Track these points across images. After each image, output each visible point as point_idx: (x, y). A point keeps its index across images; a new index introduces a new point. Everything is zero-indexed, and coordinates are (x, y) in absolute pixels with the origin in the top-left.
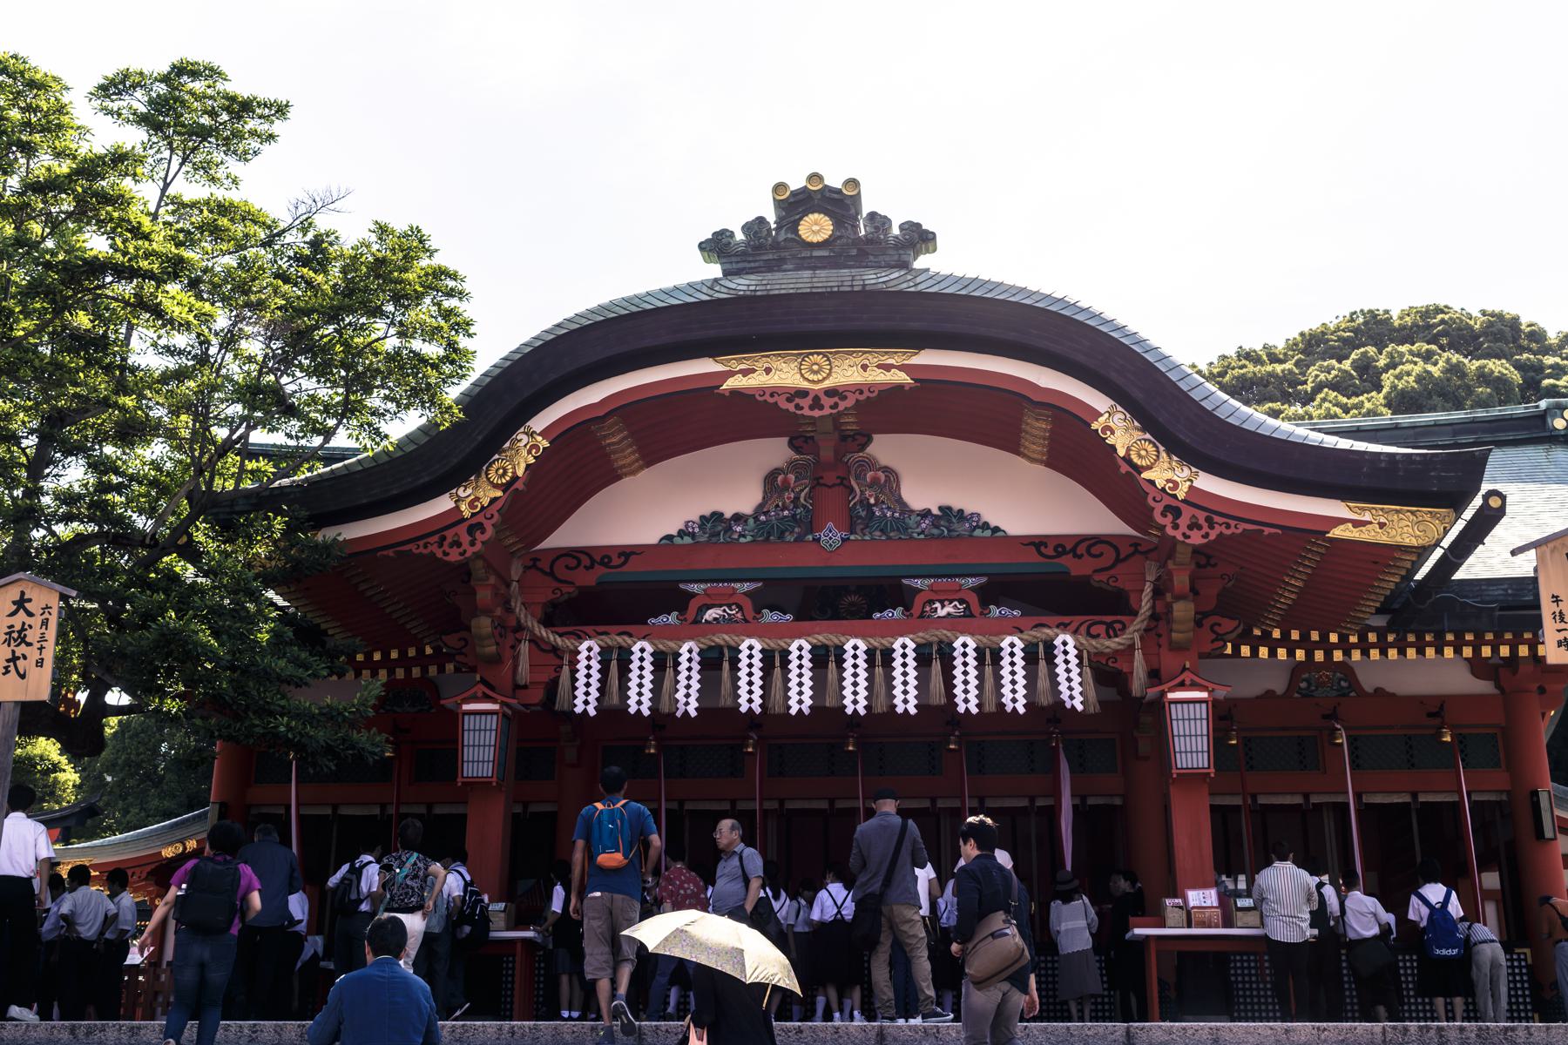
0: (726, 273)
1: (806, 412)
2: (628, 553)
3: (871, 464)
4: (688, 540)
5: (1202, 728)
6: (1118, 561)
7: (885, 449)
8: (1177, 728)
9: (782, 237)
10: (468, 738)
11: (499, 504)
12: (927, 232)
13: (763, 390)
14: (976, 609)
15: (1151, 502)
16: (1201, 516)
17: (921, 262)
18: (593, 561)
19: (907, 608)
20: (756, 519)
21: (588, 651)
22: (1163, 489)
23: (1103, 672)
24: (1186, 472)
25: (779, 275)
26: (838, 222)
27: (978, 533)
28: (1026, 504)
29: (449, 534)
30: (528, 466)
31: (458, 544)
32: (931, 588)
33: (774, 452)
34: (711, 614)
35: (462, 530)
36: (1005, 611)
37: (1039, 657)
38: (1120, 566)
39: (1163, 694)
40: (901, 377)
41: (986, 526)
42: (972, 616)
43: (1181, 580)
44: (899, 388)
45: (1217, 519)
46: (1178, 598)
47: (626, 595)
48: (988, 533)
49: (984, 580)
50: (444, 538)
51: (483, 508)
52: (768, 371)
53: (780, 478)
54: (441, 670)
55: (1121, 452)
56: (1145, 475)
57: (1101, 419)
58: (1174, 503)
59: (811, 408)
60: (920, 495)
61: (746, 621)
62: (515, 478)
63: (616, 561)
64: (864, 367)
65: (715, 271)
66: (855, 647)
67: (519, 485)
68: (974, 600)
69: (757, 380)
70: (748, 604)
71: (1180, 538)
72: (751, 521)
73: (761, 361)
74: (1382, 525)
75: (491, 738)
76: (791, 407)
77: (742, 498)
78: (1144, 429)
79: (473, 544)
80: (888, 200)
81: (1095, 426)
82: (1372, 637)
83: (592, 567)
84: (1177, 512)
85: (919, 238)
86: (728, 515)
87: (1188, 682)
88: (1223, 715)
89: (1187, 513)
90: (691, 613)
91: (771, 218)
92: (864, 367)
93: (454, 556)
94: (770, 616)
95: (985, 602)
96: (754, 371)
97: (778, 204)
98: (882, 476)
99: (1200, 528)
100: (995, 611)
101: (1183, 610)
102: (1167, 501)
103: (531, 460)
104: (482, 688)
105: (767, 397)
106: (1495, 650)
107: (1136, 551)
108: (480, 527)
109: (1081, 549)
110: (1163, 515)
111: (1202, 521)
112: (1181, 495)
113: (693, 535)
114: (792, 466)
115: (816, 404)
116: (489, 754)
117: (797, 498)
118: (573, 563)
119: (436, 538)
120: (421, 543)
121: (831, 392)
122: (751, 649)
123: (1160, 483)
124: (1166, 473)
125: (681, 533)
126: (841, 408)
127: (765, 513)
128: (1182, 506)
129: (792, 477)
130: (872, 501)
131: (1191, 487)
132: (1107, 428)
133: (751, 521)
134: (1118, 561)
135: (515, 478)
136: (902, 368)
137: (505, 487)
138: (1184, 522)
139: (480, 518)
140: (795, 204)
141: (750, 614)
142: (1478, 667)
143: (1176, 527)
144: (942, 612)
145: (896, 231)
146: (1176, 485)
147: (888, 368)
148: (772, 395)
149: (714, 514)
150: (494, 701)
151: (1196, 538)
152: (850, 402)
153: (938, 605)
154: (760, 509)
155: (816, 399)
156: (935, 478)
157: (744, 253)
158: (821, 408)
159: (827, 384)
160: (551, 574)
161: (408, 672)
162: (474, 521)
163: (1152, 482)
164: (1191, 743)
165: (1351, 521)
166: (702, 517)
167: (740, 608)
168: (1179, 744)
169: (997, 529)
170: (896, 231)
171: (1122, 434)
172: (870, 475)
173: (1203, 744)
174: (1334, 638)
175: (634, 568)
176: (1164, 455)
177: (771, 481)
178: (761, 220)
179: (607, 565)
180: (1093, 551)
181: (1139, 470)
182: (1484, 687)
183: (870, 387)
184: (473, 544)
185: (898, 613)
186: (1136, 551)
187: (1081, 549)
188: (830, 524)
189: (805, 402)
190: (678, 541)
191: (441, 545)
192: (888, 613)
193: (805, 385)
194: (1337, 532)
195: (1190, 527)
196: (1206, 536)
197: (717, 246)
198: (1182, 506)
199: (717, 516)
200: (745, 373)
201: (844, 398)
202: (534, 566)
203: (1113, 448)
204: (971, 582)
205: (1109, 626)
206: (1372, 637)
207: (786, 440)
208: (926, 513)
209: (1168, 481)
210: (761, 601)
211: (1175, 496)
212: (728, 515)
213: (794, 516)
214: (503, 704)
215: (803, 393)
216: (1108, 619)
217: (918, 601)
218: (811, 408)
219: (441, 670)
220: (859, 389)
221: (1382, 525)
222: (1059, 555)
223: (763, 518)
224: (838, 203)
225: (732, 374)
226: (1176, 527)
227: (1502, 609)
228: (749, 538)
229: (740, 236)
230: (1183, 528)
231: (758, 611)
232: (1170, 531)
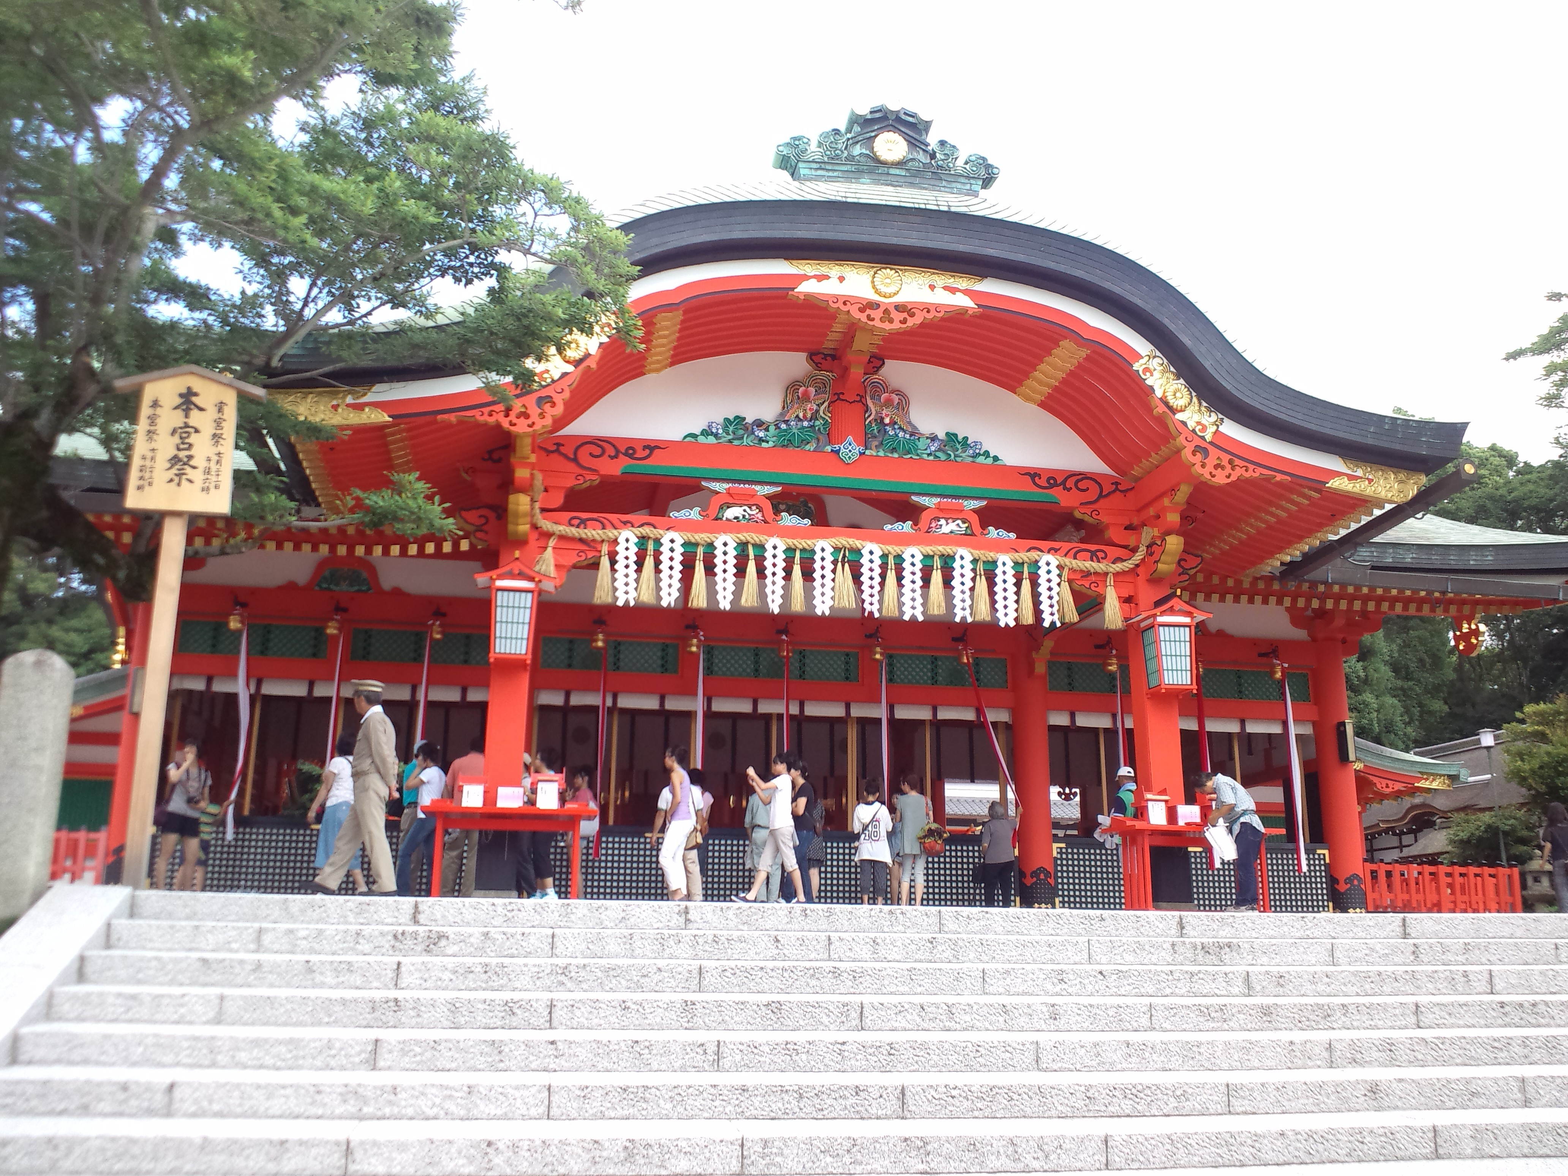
1: (877, 323)
2: (652, 447)
3: (884, 387)
4: (711, 440)
5: (1186, 649)
6: (1101, 496)
7: (895, 372)
8: (1165, 648)
10: (500, 614)
11: (568, 381)
12: (990, 166)
13: (837, 298)
14: (977, 529)
16: (1225, 458)
18: (618, 451)
19: (916, 523)
20: (777, 427)
22: (1194, 431)
24: (1214, 417)
27: (981, 460)
28: (1025, 440)
31: (526, 416)
32: (939, 507)
33: (795, 363)
36: (1003, 533)
37: (1027, 576)
38: (1102, 501)
40: (965, 302)
41: (987, 454)
42: (973, 534)
43: (1173, 518)
45: (1237, 462)
47: (644, 488)
48: (990, 461)
49: (984, 503)
51: (553, 381)
52: (841, 279)
53: (801, 390)
54: (386, 552)
55: (1159, 393)
56: (1179, 416)
57: (1142, 361)
58: (1203, 444)
60: (929, 420)
61: (766, 522)
62: (587, 356)
63: (640, 454)
64: (932, 287)
70: (768, 506)
72: (772, 428)
73: (834, 270)
74: (1370, 481)
76: (863, 317)
77: (764, 407)
78: (1178, 376)
79: (542, 416)
80: (956, 130)
81: (1136, 366)
82: (1261, 585)
83: (616, 457)
86: (749, 420)
87: (1176, 608)
88: (1205, 641)
90: (713, 511)
94: (788, 520)
95: (984, 526)
96: (827, 277)
98: (896, 399)
99: (1223, 468)
101: (1174, 543)
103: (605, 339)
105: (840, 305)
106: (1308, 602)
107: (1117, 489)
108: (549, 400)
109: (1070, 483)
110: (1194, 453)
111: (1225, 462)
112: (1209, 437)
113: (716, 436)
114: (809, 380)
117: (817, 411)
118: (597, 451)
119: (501, 407)
120: (486, 410)
121: (900, 308)
122: (776, 548)
123: (1191, 424)
124: (1195, 417)
125: (705, 433)
126: (911, 322)
127: (786, 422)
128: (1210, 448)
129: (812, 390)
130: (887, 421)
131: (1217, 432)
132: (1146, 370)
133: (772, 428)
134: (1101, 496)
135: (587, 356)
136: (966, 292)
137: (577, 363)
138: (1211, 461)
142: (1297, 618)
143: (1203, 466)
145: (960, 162)
147: (953, 290)
148: (845, 303)
149: (737, 417)
151: (1220, 479)
152: (917, 320)
153: (943, 522)
155: (886, 311)
156: (941, 407)
158: (891, 321)
160: (575, 460)
161: (351, 549)
162: (543, 393)
163: (1184, 423)
165: (1344, 477)
166: (727, 420)
167: (761, 510)
168: (1166, 663)
169: (996, 458)
170: (960, 162)
172: (884, 396)
173: (1186, 663)
174: (1230, 583)
175: (656, 466)
176: (1195, 400)
177: (793, 391)
178: (836, 132)
179: (631, 457)
180: (1080, 485)
181: (1174, 411)
182: (1301, 634)
183: (937, 307)
184: (542, 416)
186: (1117, 489)
187: (1070, 483)
188: (850, 438)
189: (877, 314)
190: (702, 439)
191: (507, 416)
193: (876, 298)
194: (1334, 483)
195: (1216, 467)
196: (1228, 477)
198: (1210, 448)
199: (739, 420)
201: (912, 315)
202: (557, 451)
206: (1261, 585)
207: (803, 355)
208: (933, 438)
209: (1199, 423)
211: (1203, 438)
212: (749, 420)
213: (813, 426)
215: (872, 305)
217: (925, 517)
219: (386, 552)
221: (1370, 481)
222: (1051, 486)
223: (784, 426)
224: (912, 127)
225: (806, 278)
226: (1203, 466)
227: (1373, 568)
228: (771, 444)
230: (1209, 468)
232: (1198, 469)
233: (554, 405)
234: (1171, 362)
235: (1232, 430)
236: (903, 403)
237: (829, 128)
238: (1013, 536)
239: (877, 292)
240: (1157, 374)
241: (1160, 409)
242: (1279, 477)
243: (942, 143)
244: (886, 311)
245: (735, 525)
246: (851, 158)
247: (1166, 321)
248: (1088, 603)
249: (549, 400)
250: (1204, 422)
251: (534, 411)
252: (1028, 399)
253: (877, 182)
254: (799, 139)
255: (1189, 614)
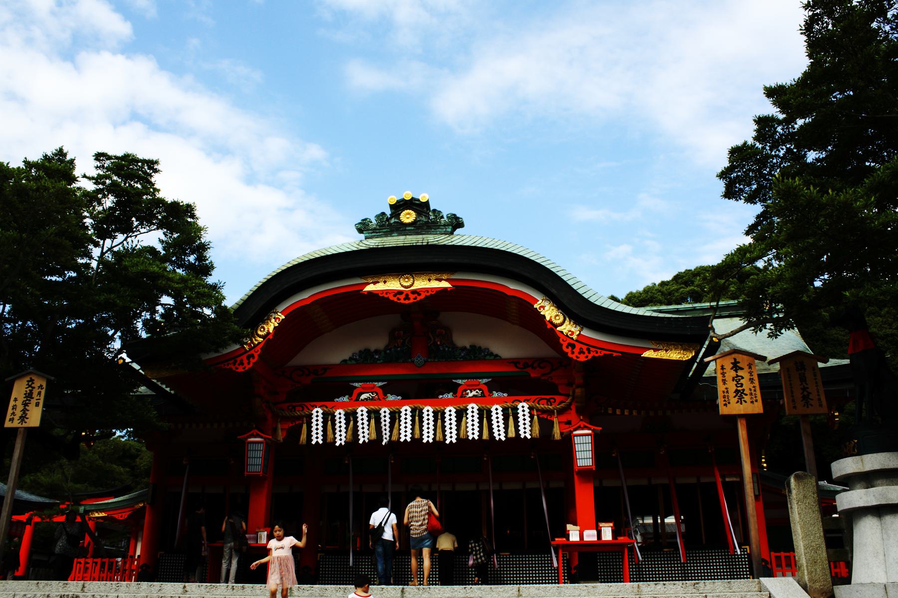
0: (366, 238)
1: (402, 301)
2: (327, 368)
4: (353, 362)
5: (589, 447)
7: (446, 318)
8: (578, 448)
9: (393, 221)
11: (260, 346)
14: (487, 393)
15: (561, 341)
16: (585, 348)
17: (458, 231)
19: (455, 393)
21: (317, 413)
23: (544, 421)
24: (578, 328)
25: (389, 238)
26: (419, 213)
27: (488, 357)
29: (239, 359)
30: (275, 328)
31: (242, 363)
34: (363, 396)
35: (244, 357)
36: (500, 394)
39: (572, 432)
40: (445, 284)
44: (445, 289)
45: (592, 349)
46: (577, 387)
50: (236, 361)
52: (385, 282)
55: (548, 318)
56: (559, 329)
59: (405, 299)
60: (463, 341)
62: (268, 333)
64: (429, 280)
65: (362, 236)
66: (428, 411)
67: (271, 337)
68: (485, 388)
69: (380, 287)
70: (380, 391)
71: (575, 358)
75: (260, 454)
76: (395, 299)
77: (378, 343)
79: (249, 363)
80: (443, 204)
81: (536, 306)
84: (573, 346)
85: (456, 223)
86: (372, 349)
89: (578, 346)
91: (388, 212)
92: (429, 280)
93: (241, 369)
94: (391, 398)
95: (491, 392)
97: (392, 206)
100: (495, 394)
102: (569, 341)
104: (255, 431)
108: (252, 356)
110: (567, 347)
112: (575, 337)
113: (356, 360)
115: (407, 297)
116: (260, 461)
119: (231, 362)
121: (414, 292)
123: (565, 331)
124: (568, 328)
125: (351, 359)
126: (419, 298)
127: (390, 350)
135: (268, 333)
136: (446, 280)
138: (576, 350)
139: (252, 352)
140: (399, 206)
141: (381, 396)
143: (573, 353)
144: (470, 395)
146: (573, 333)
147: (440, 280)
150: (261, 437)
151: (582, 358)
152: (422, 297)
154: (387, 347)
155: (407, 295)
157: (375, 229)
158: (409, 299)
159: (412, 288)
163: (562, 332)
164: (584, 453)
168: (579, 455)
169: (497, 355)
171: (549, 312)
177: (393, 335)
178: (383, 214)
181: (556, 326)
184: (249, 363)
185: (450, 396)
189: (402, 297)
190: (349, 362)
192: (445, 396)
193: (402, 289)
195: (580, 353)
197: (363, 227)
198: (577, 344)
199: (367, 351)
200: (375, 283)
201: (419, 295)
203: (544, 316)
204: (485, 381)
205: (548, 400)
208: (464, 348)
210: (386, 390)
212: (372, 349)
214: (265, 438)
215: (400, 292)
216: (548, 397)
217: (460, 390)
218: (405, 299)
220: (427, 290)
225: (369, 284)
226: (573, 353)
229: (374, 222)
230: (576, 353)
231: (385, 394)
232: (570, 355)
233: (254, 357)
234: (554, 302)
235: (586, 333)
236: (447, 334)
237: (379, 213)
238: (505, 395)
239: (402, 286)
240: (546, 308)
241: (549, 326)
242: (615, 354)
243: (434, 211)
244: (407, 295)
245: (365, 402)
246: (390, 225)
247: (542, 283)
248: (546, 426)
249: (252, 356)
250: (573, 330)
251: (245, 362)
252: (513, 323)
253: (400, 235)
254: (365, 219)
255: (589, 429)
